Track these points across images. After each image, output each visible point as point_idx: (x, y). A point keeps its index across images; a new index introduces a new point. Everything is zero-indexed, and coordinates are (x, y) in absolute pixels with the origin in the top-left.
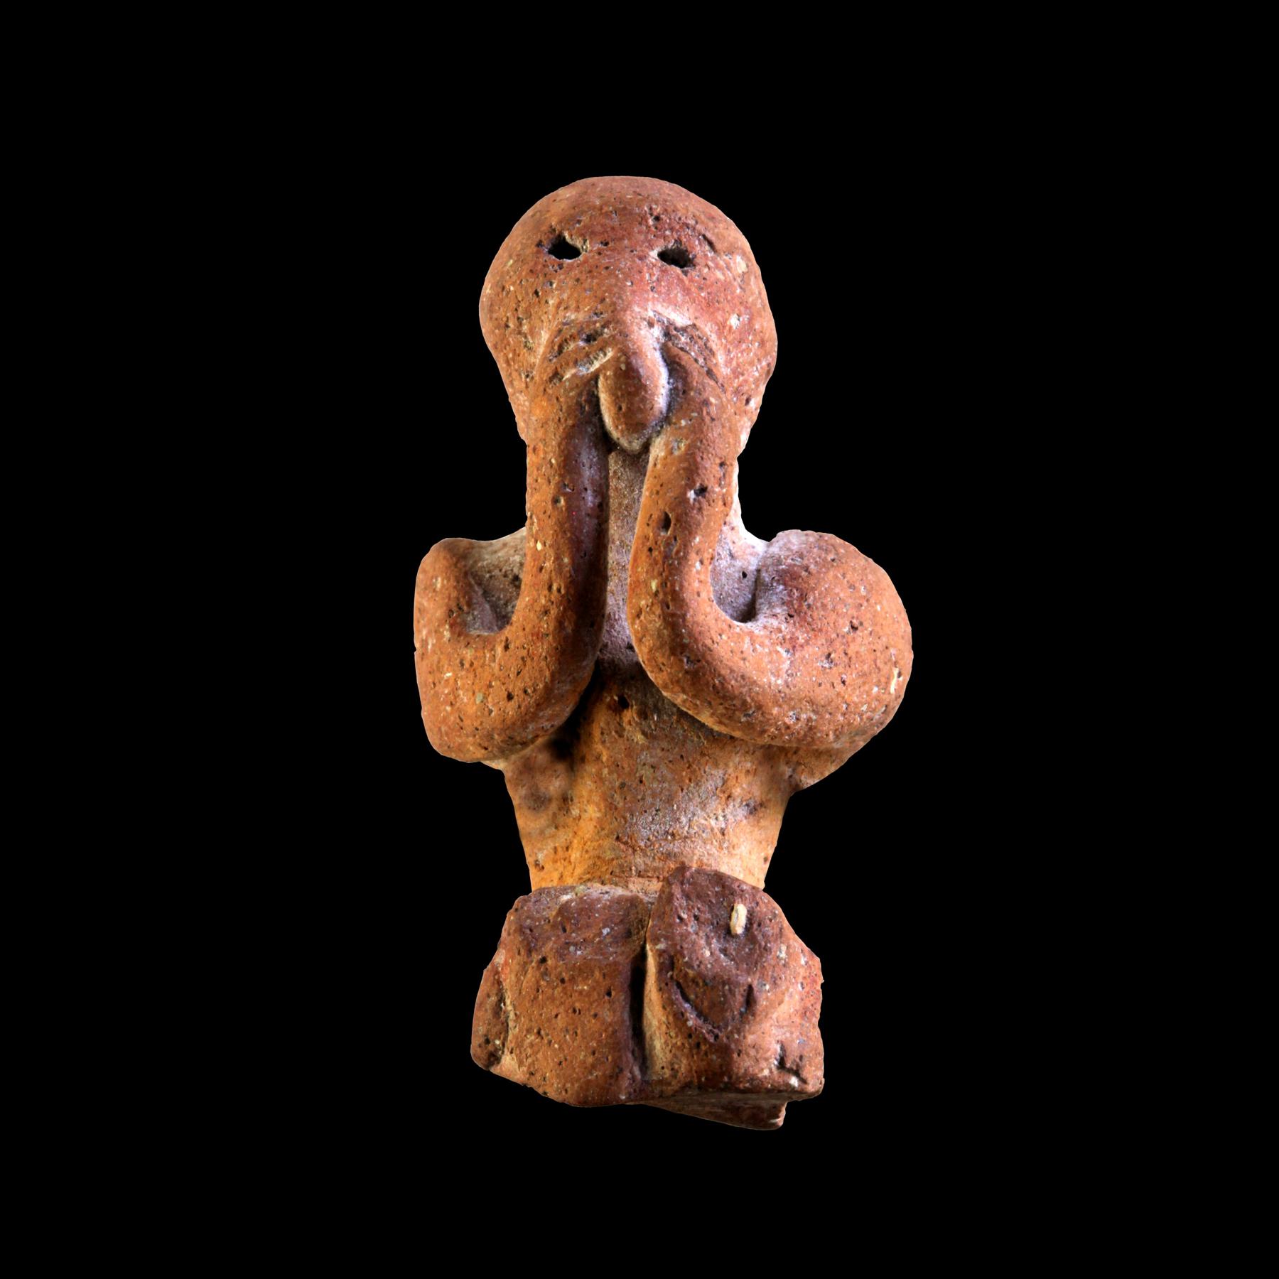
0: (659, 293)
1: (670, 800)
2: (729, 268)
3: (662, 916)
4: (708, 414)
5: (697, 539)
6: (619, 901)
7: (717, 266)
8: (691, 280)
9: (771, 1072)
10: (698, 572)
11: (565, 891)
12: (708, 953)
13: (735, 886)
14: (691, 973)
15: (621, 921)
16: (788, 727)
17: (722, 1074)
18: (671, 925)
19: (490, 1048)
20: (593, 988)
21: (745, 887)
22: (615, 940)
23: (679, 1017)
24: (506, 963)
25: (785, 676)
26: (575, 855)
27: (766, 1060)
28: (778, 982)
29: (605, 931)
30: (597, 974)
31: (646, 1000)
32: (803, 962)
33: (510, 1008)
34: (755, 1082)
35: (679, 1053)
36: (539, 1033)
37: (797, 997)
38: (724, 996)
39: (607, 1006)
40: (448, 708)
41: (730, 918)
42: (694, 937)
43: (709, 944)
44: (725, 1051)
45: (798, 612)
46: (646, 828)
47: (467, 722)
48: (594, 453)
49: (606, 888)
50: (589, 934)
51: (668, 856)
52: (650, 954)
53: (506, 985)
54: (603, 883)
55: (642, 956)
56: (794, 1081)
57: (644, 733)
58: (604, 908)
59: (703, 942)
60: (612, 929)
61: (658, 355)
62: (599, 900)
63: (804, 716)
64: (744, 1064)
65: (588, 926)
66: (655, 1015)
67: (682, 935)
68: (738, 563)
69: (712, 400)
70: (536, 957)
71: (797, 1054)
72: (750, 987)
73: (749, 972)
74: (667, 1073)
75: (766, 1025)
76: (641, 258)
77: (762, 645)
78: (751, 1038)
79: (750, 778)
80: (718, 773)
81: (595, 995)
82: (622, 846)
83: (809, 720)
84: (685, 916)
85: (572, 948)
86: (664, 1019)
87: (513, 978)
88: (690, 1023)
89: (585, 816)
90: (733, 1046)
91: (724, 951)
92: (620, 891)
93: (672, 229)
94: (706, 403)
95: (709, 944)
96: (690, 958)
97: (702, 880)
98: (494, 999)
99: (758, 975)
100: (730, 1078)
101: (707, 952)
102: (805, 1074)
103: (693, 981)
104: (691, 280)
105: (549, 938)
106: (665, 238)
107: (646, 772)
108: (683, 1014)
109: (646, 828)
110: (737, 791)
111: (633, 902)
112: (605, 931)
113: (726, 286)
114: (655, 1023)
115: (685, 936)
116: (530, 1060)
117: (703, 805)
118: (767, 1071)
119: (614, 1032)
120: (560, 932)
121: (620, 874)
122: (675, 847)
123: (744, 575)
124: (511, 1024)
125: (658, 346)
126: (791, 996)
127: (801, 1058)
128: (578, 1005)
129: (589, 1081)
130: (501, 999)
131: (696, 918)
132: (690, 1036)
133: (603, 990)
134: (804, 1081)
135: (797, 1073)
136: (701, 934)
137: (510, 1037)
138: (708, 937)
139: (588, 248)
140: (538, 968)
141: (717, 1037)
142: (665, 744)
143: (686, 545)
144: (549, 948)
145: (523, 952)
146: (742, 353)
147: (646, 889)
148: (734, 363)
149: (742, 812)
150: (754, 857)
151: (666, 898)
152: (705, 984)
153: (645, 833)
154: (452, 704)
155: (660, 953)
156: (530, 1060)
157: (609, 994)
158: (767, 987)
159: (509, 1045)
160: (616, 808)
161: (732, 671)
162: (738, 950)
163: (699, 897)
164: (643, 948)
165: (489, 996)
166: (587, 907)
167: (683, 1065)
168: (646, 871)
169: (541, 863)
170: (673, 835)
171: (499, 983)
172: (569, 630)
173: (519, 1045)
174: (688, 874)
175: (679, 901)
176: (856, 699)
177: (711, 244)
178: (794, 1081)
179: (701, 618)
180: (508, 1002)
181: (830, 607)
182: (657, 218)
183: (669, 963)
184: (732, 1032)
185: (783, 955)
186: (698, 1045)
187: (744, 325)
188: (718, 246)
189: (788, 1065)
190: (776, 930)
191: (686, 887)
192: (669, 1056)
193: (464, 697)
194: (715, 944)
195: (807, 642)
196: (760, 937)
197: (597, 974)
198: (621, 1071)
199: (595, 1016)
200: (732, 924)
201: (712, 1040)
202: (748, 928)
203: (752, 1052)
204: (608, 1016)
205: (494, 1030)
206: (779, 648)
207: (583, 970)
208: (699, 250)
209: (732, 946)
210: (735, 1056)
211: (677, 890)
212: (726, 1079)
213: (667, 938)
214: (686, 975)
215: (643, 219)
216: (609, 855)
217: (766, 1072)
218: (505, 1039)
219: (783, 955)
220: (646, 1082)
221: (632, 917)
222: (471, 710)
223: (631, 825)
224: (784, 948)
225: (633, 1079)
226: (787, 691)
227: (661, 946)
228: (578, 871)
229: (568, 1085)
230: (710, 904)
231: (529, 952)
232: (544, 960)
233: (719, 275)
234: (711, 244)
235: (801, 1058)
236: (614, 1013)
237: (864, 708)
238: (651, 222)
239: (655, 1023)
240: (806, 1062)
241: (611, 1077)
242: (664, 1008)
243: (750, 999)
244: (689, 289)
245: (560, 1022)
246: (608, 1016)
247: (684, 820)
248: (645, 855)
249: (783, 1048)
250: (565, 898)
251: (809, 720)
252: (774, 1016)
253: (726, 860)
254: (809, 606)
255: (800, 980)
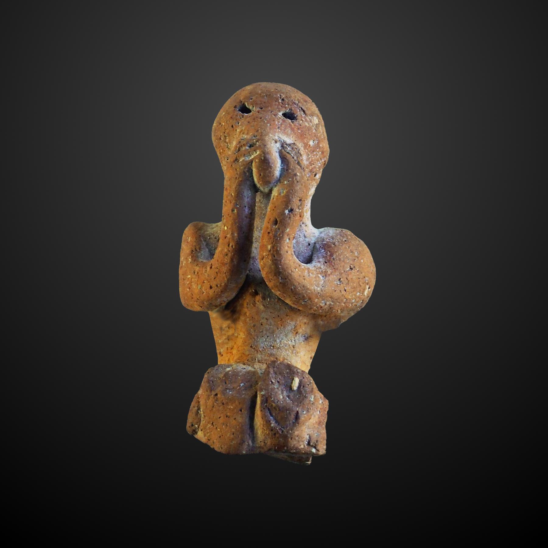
0: (281, 130)
1: (273, 332)
2: (311, 121)
3: (264, 380)
4: (296, 179)
5: (288, 230)
6: (248, 372)
7: (306, 120)
8: (295, 125)
9: (304, 446)
10: (288, 243)
11: (228, 367)
12: (281, 397)
13: (295, 370)
14: (274, 404)
15: (249, 381)
16: (321, 307)
17: (284, 446)
18: (268, 385)
19: (193, 428)
20: (235, 408)
21: (299, 371)
22: (245, 389)
23: (268, 422)
24: (202, 395)
25: (321, 287)
26: (234, 351)
27: (303, 441)
28: (309, 410)
29: (242, 385)
30: (237, 402)
31: (256, 415)
32: (321, 402)
33: (202, 413)
34: (298, 450)
35: (267, 437)
36: (212, 423)
37: (317, 416)
38: (287, 415)
39: (240, 415)
40: (188, 290)
41: (292, 383)
42: (276, 390)
43: (282, 393)
44: (285, 437)
45: (329, 261)
46: (262, 343)
47: (194, 296)
48: (249, 192)
49: (244, 367)
50: (235, 385)
51: (271, 355)
52: (258, 396)
53: (201, 403)
54: (244, 364)
55: (256, 396)
56: (314, 450)
57: (264, 306)
58: (242, 375)
59: (280, 392)
60: (245, 384)
61: (277, 155)
62: (241, 372)
63: (328, 303)
64: (293, 443)
65: (235, 382)
66: (259, 421)
67: (271, 389)
68: (307, 240)
69: (298, 174)
70: (213, 393)
71: (315, 440)
72: (298, 412)
73: (297, 406)
74: (262, 444)
75: (303, 428)
76: (274, 115)
77: (312, 274)
78: (296, 433)
79: (306, 326)
80: (293, 323)
81: (236, 410)
82: (253, 350)
83: (330, 304)
84: (274, 381)
85: (228, 391)
86: (262, 422)
87: (204, 401)
88: (272, 425)
89: (239, 337)
90: (289, 436)
91: (288, 396)
92: (250, 368)
93: (288, 105)
94: (295, 175)
95: (282, 393)
96: (274, 399)
97: (282, 367)
98: (196, 408)
99: (301, 407)
100: (287, 448)
101: (281, 396)
102: (318, 448)
103: (275, 408)
104: (295, 125)
105: (219, 386)
106: (285, 108)
107: (264, 321)
108: (269, 421)
109: (262, 343)
110: (300, 331)
111: (254, 373)
112: (242, 385)
113: (309, 129)
114: (259, 424)
115: (273, 389)
116: (208, 434)
117: (286, 336)
118: (303, 446)
119: (242, 426)
120: (224, 384)
121: (251, 361)
122: (274, 351)
123: (309, 244)
124: (202, 419)
125: (278, 151)
126: (315, 416)
127: (317, 441)
128: (228, 414)
129: (231, 445)
130: (199, 409)
131: (278, 382)
132: (272, 430)
133: (239, 409)
134: (318, 450)
135: (315, 448)
136: (280, 389)
137: (201, 424)
138: (282, 390)
139: (255, 109)
140: (214, 398)
141: (283, 431)
142: (272, 311)
143: (283, 232)
144: (219, 390)
145: (208, 390)
146: (314, 155)
147: (260, 368)
148: (310, 160)
149: (302, 339)
150: (306, 357)
151: (267, 373)
152: (279, 410)
153: (262, 345)
154: (189, 288)
155: (263, 396)
156: (208, 434)
157: (241, 411)
158: (305, 412)
159: (201, 427)
160: (251, 335)
161: (299, 284)
162: (294, 396)
163: (280, 374)
164: (256, 393)
165: (194, 407)
166: (235, 374)
167: (269, 442)
168: (262, 360)
169: (222, 353)
170: (273, 347)
171: (199, 402)
172: (235, 263)
173: (205, 428)
174: (276, 364)
175: (272, 374)
176: (350, 297)
177: (304, 111)
178: (314, 450)
179: (287, 262)
180: (201, 410)
181: (342, 260)
182: (283, 100)
183: (266, 400)
184: (289, 430)
185: (312, 400)
186: (275, 434)
187: (315, 144)
188: (307, 112)
189: (311, 444)
190: (311, 389)
191: (275, 369)
192: (263, 437)
193: (194, 286)
194: (285, 393)
195: (331, 273)
196: (303, 392)
197: (237, 402)
198: (244, 442)
199: (235, 419)
200: (292, 385)
201: (281, 433)
202: (299, 387)
203: (297, 438)
204: (240, 420)
205: (195, 421)
206: (319, 275)
207: (231, 400)
208: (299, 113)
209: (292, 395)
210: (290, 439)
211: (271, 371)
212: (285, 448)
213: (265, 390)
214: (272, 405)
215: (277, 100)
216: (247, 353)
217: (302, 446)
218: (199, 425)
219: (312, 400)
220: (253, 447)
221: (253, 379)
222: (196, 291)
223: (257, 342)
224: (313, 397)
225: (249, 445)
226: (322, 293)
227: (262, 393)
228: (235, 358)
229: (223, 446)
230: (284, 377)
231: (211, 391)
232: (216, 395)
233: (307, 124)
234: (304, 111)
235: (317, 441)
236: (242, 418)
237: (353, 301)
238: (280, 101)
239: (259, 424)
240: (319, 443)
241: (240, 444)
242: (262, 418)
243: (297, 417)
244: (293, 129)
245: (221, 421)
246: (240, 420)
247: (278, 341)
248: (262, 354)
249: (310, 437)
250: (228, 369)
251: (330, 304)
252: (307, 424)
253: (294, 358)
254: (334, 259)
255: (319, 410)
